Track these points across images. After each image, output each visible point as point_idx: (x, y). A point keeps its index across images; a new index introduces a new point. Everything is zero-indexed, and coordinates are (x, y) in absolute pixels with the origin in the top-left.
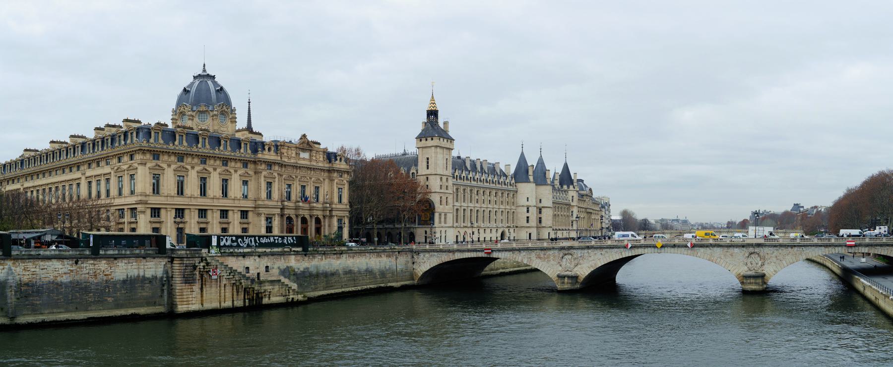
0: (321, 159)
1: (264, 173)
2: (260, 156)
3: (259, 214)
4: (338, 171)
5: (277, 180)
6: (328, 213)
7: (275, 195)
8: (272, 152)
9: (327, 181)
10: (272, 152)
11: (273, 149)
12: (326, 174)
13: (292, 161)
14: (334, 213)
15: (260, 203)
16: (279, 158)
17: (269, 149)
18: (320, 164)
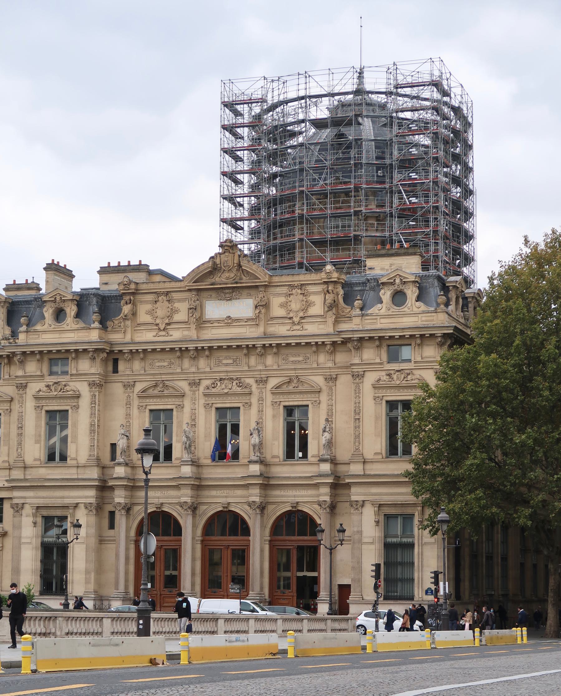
0: (317, 309)
1: (34, 387)
2: (22, 338)
3: (18, 509)
4: (380, 340)
5: (85, 402)
6: (325, 494)
7: (80, 447)
8: (70, 321)
9: (344, 380)
10: (70, 321)
11: (71, 310)
12: (341, 358)
13: (176, 335)
14: (356, 494)
15: (17, 474)
16: (94, 335)
17: (59, 315)
18: (312, 328)
